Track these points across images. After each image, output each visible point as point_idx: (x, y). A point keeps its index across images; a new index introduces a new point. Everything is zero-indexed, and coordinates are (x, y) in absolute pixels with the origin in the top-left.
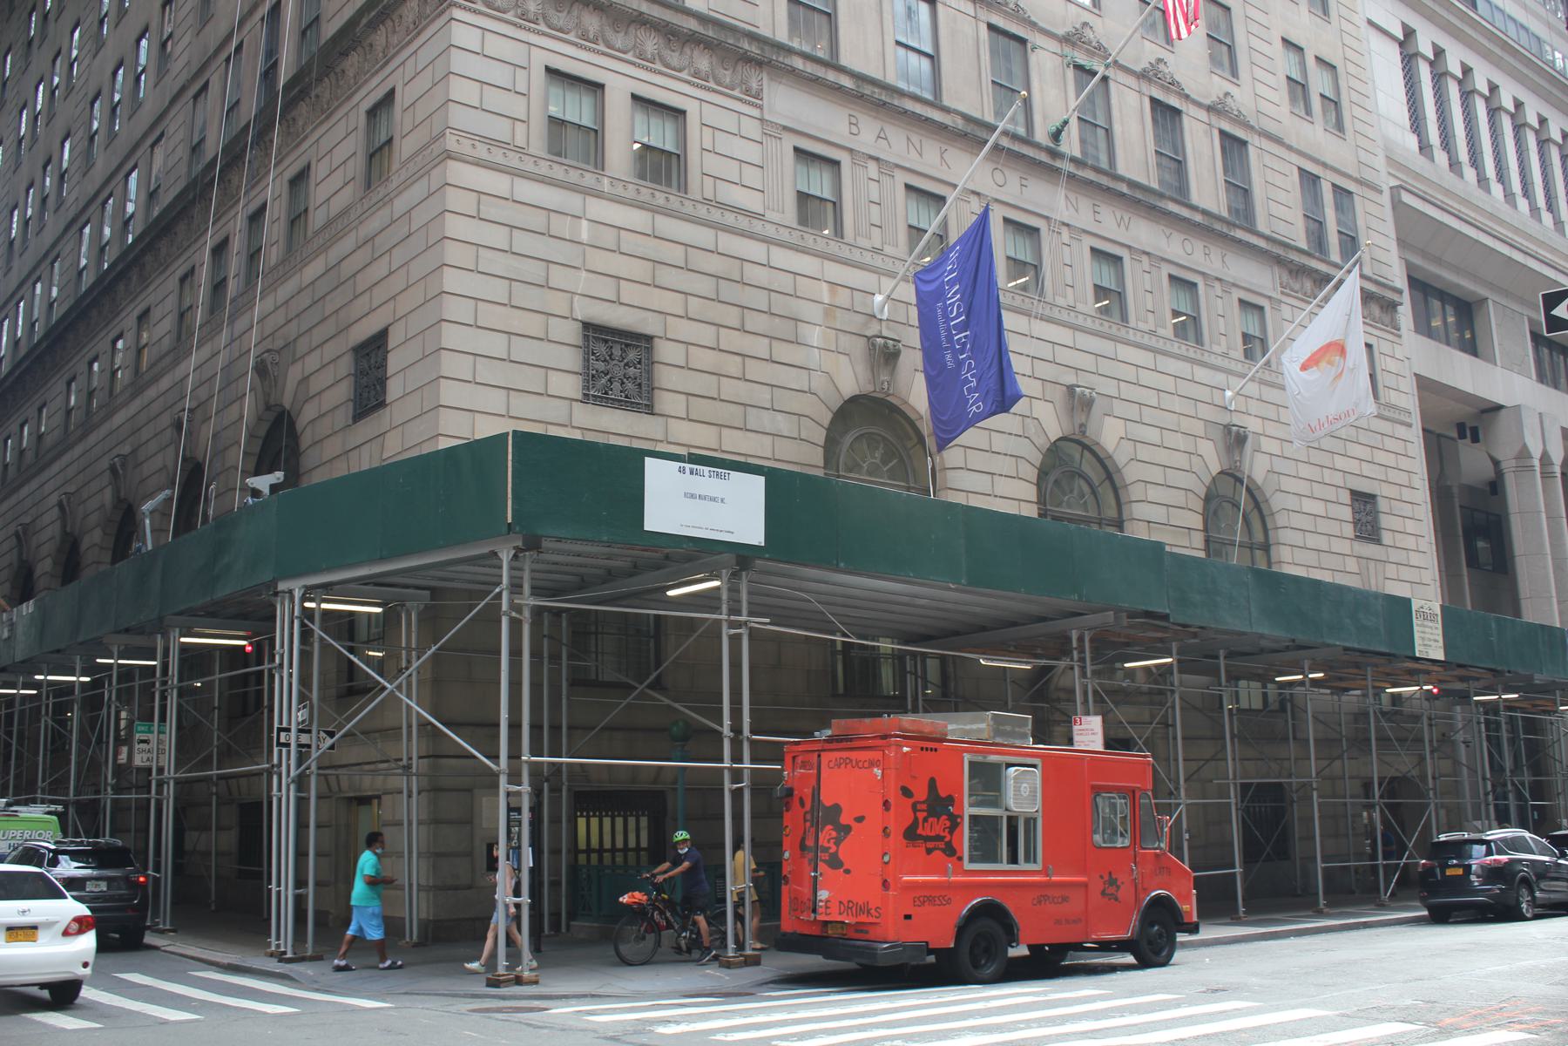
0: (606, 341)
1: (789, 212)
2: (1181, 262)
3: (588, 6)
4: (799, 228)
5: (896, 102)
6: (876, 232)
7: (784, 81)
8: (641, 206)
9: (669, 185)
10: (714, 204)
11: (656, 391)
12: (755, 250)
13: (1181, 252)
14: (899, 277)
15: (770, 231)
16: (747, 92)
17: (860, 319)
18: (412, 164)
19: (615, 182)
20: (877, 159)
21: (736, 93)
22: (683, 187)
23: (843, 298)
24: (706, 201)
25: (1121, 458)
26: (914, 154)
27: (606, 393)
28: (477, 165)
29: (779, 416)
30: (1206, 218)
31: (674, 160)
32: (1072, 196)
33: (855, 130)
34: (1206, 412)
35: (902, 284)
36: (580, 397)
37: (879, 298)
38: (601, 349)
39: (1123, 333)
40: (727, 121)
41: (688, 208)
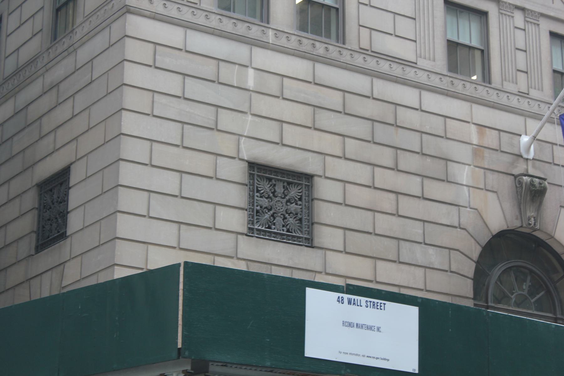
0: (270, 180)
4: (449, 74)
6: (522, 77)
9: (328, 36)
10: (369, 53)
11: (315, 226)
14: (544, 119)
15: (422, 77)
17: (507, 158)
18: (94, 17)
19: (279, 34)
20: (523, 9)
22: (341, 38)
23: (491, 139)
24: (363, 51)
27: (269, 227)
28: (154, 18)
29: (431, 250)
31: (333, 12)
35: (547, 125)
36: (245, 231)
37: (525, 139)
38: (265, 187)
41: (346, 57)
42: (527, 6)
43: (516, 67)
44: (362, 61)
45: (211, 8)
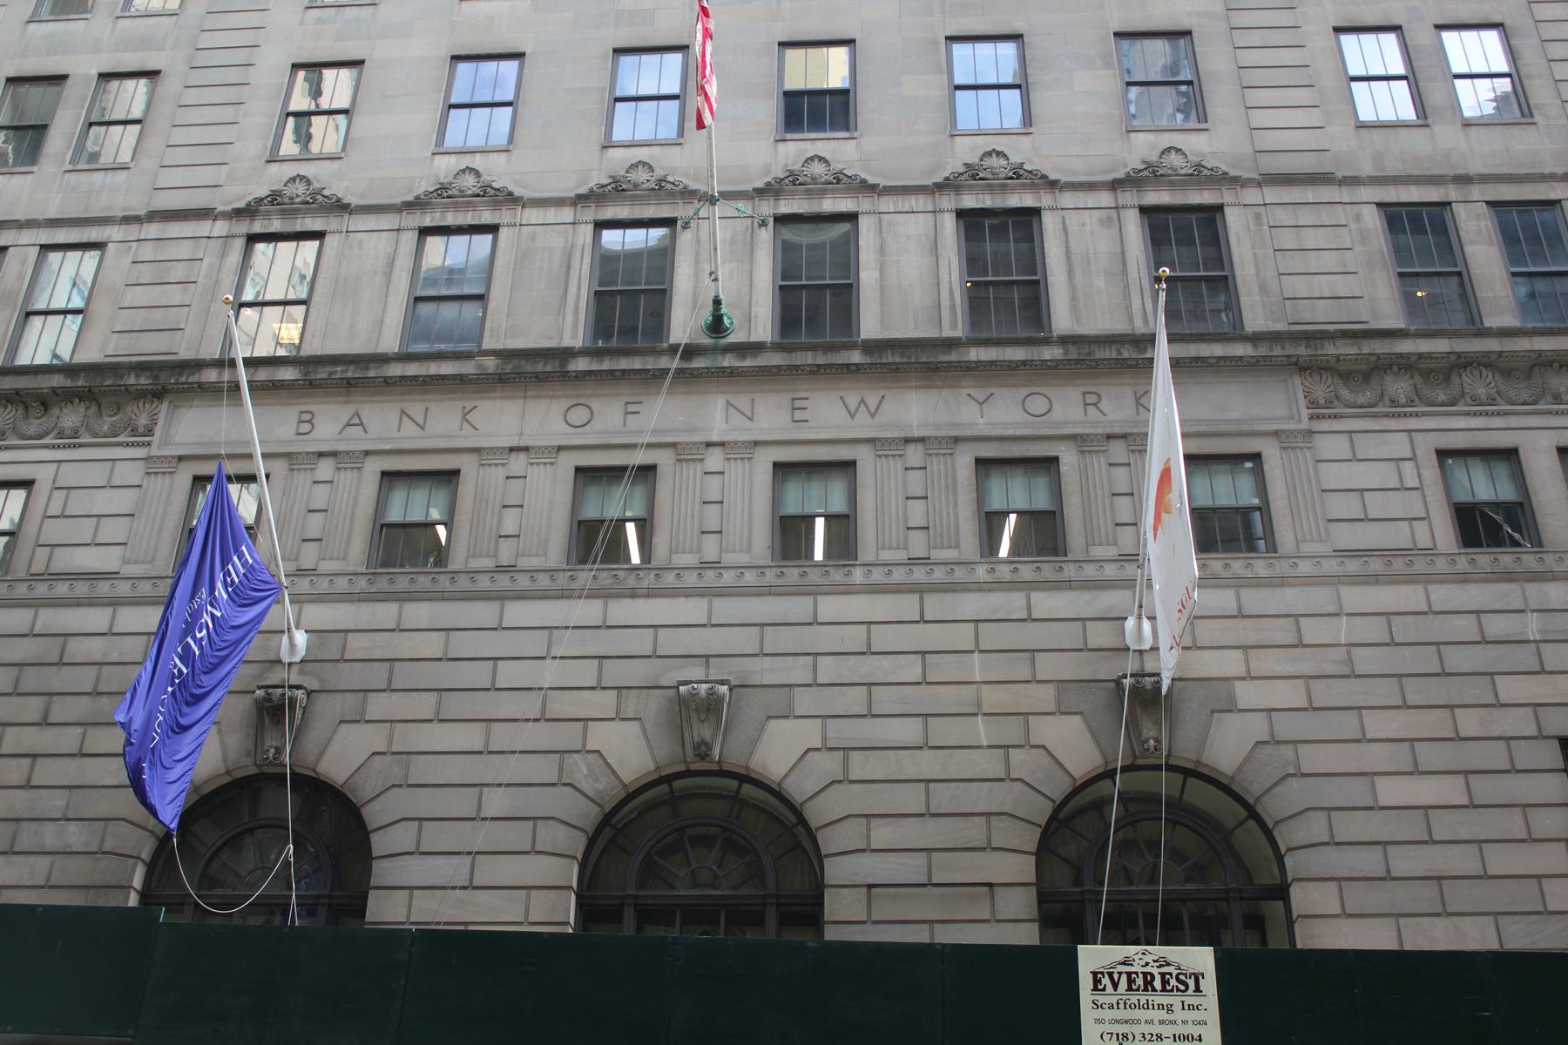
1: (1444, 532)
2: (1019, 432)
3: (72, 402)
4: (1462, 551)
5: (371, 374)
7: (195, 403)
8: (385, 597)
12: (96, 619)
13: (1020, 416)
16: (134, 432)
21: (120, 439)
25: (799, 789)
26: (409, 428)
29: (73, 827)
32: (742, 401)
33: (305, 427)
34: (1066, 666)
39: (444, 583)
40: (96, 475)
42: (530, 443)
43: (1113, 518)
44: (508, 583)
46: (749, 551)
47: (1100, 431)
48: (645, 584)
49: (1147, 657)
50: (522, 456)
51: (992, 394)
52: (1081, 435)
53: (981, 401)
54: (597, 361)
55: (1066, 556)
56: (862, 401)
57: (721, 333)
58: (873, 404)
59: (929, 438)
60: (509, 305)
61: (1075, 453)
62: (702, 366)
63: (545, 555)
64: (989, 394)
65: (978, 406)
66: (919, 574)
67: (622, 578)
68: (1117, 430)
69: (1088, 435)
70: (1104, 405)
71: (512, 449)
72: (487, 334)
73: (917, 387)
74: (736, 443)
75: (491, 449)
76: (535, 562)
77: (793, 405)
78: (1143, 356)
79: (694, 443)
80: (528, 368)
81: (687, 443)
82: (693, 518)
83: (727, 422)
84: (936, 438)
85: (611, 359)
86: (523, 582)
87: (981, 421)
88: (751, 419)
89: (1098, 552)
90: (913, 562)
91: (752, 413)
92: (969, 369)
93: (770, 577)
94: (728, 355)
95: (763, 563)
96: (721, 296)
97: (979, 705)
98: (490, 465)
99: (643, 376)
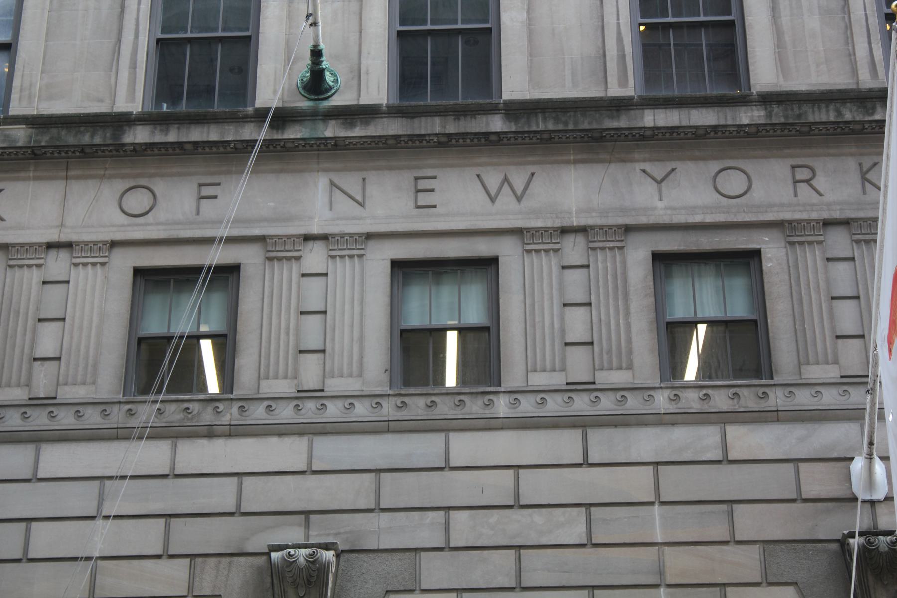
2: (709, 219)
13: (708, 197)
30: (776, 109)
32: (350, 182)
42: (74, 237)
43: (833, 328)
45: (379, 389)
46: (360, 375)
47: (814, 216)
48: (226, 419)
49: (881, 510)
50: (64, 254)
51: (673, 170)
52: (790, 222)
53: (659, 179)
54: (161, 130)
55: (772, 378)
56: (506, 180)
57: (322, 93)
58: (519, 183)
59: (592, 227)
60: (44, 58)
61: (783, 244)
62: (298, 136)
63: (94, 383)
64: (669, 169)
65: (655, 185)
66: (581, 404)
67: (195, 412)
68: (837, 215)
69: (799, 222)
70: (820, 182)
71: (50, 246)
72: (15, 96)
73: (575, 162)
74: (342, 236)
75: (22, 245)
76: (80, 393)
77: (794, 176)
78: (870, 118)
79: (289, 237)
80: (70, 138)
81: (280, 237)
82: (287, 334)
83: (331, 209)
84: (601, 227)
85: (179, 128)
86: (66, 419)
87: (660, 205)
88: (362, 205)
89: (814, 373)
90: (573, 388)
91: (364, 196)
92: (643, 138)
93: (388, 409)
94: (332, 122)
95: (378, 390)
96: (322, 46)
97: (661, 573)
98: (21, 266)
99: (222, 150)
